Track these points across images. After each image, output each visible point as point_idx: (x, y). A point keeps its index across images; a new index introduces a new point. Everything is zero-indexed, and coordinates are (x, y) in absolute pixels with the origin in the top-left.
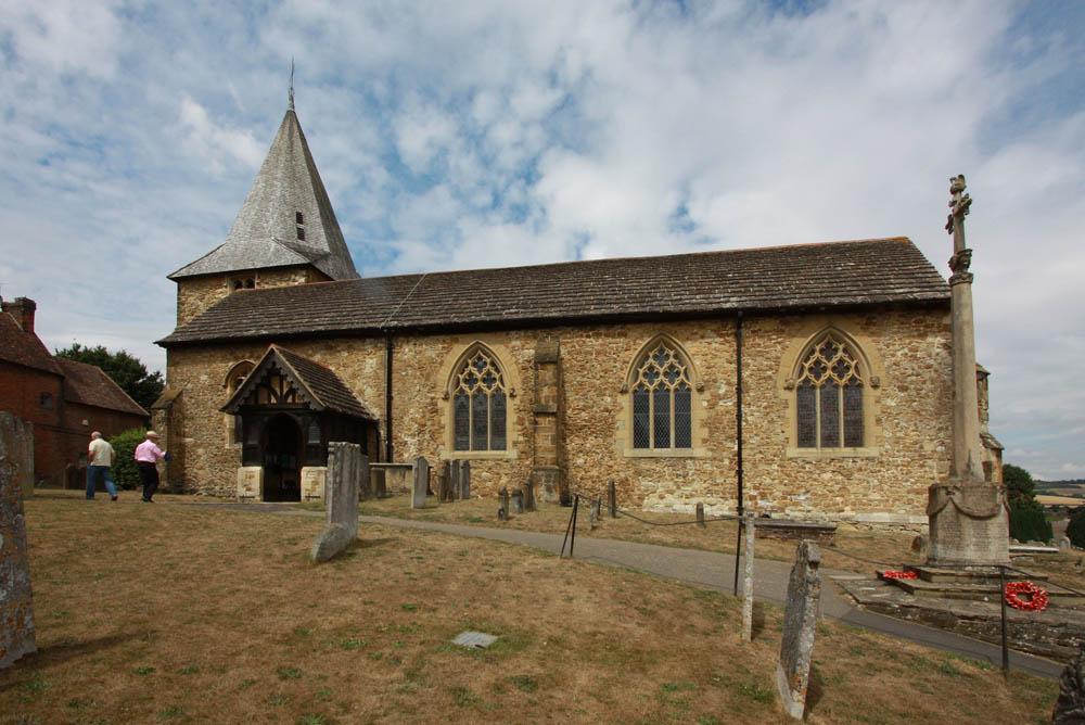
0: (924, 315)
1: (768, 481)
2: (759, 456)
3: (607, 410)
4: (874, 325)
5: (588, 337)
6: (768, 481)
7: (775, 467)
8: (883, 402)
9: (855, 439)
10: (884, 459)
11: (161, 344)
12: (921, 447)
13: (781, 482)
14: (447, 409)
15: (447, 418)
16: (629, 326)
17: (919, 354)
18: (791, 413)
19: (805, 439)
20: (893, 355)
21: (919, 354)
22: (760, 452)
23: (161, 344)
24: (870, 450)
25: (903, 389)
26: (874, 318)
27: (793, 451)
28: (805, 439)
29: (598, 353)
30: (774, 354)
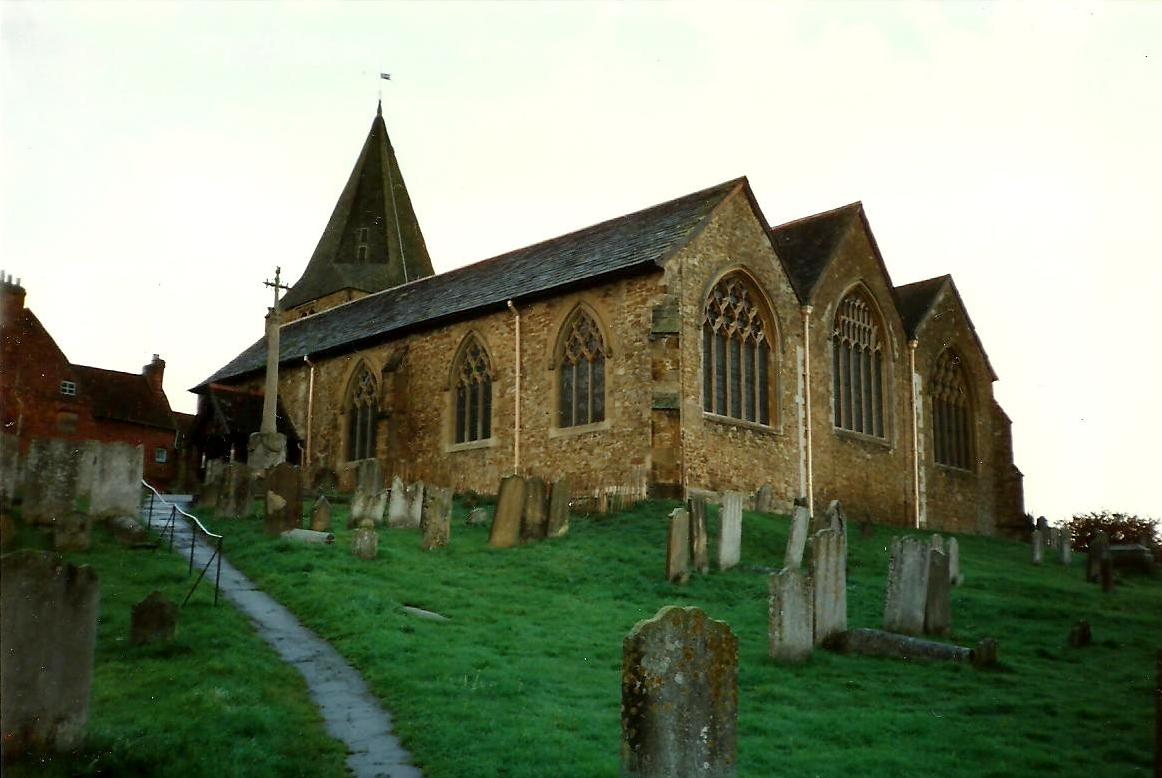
0: (645, 280)
1: (538, 464)
2: (532, 439)
3: (436, 410)
4: (610, 295)
5: (427, 341)
6: (538, 464)
7: (542, 449)
8: (615, 373)
9: (599, 417)
10: (615, 431)
11: (192, 391)
12: (641, 415)
13: (546, 464)
14: (342, 421)
15: (342, 434)
16: (452, 327)
17: (642, 319)
18: (553, 395)
19: (564, 421)
20: (622, 323)
21: (642, 319)
22: (532, 436)
23: (192, 391)
24: (606, 424)
25: (629, 356)
26: (610, 290)
27: (553, 432)
28: (564, 421)
29: (432, 356)
30: (542, 338)
